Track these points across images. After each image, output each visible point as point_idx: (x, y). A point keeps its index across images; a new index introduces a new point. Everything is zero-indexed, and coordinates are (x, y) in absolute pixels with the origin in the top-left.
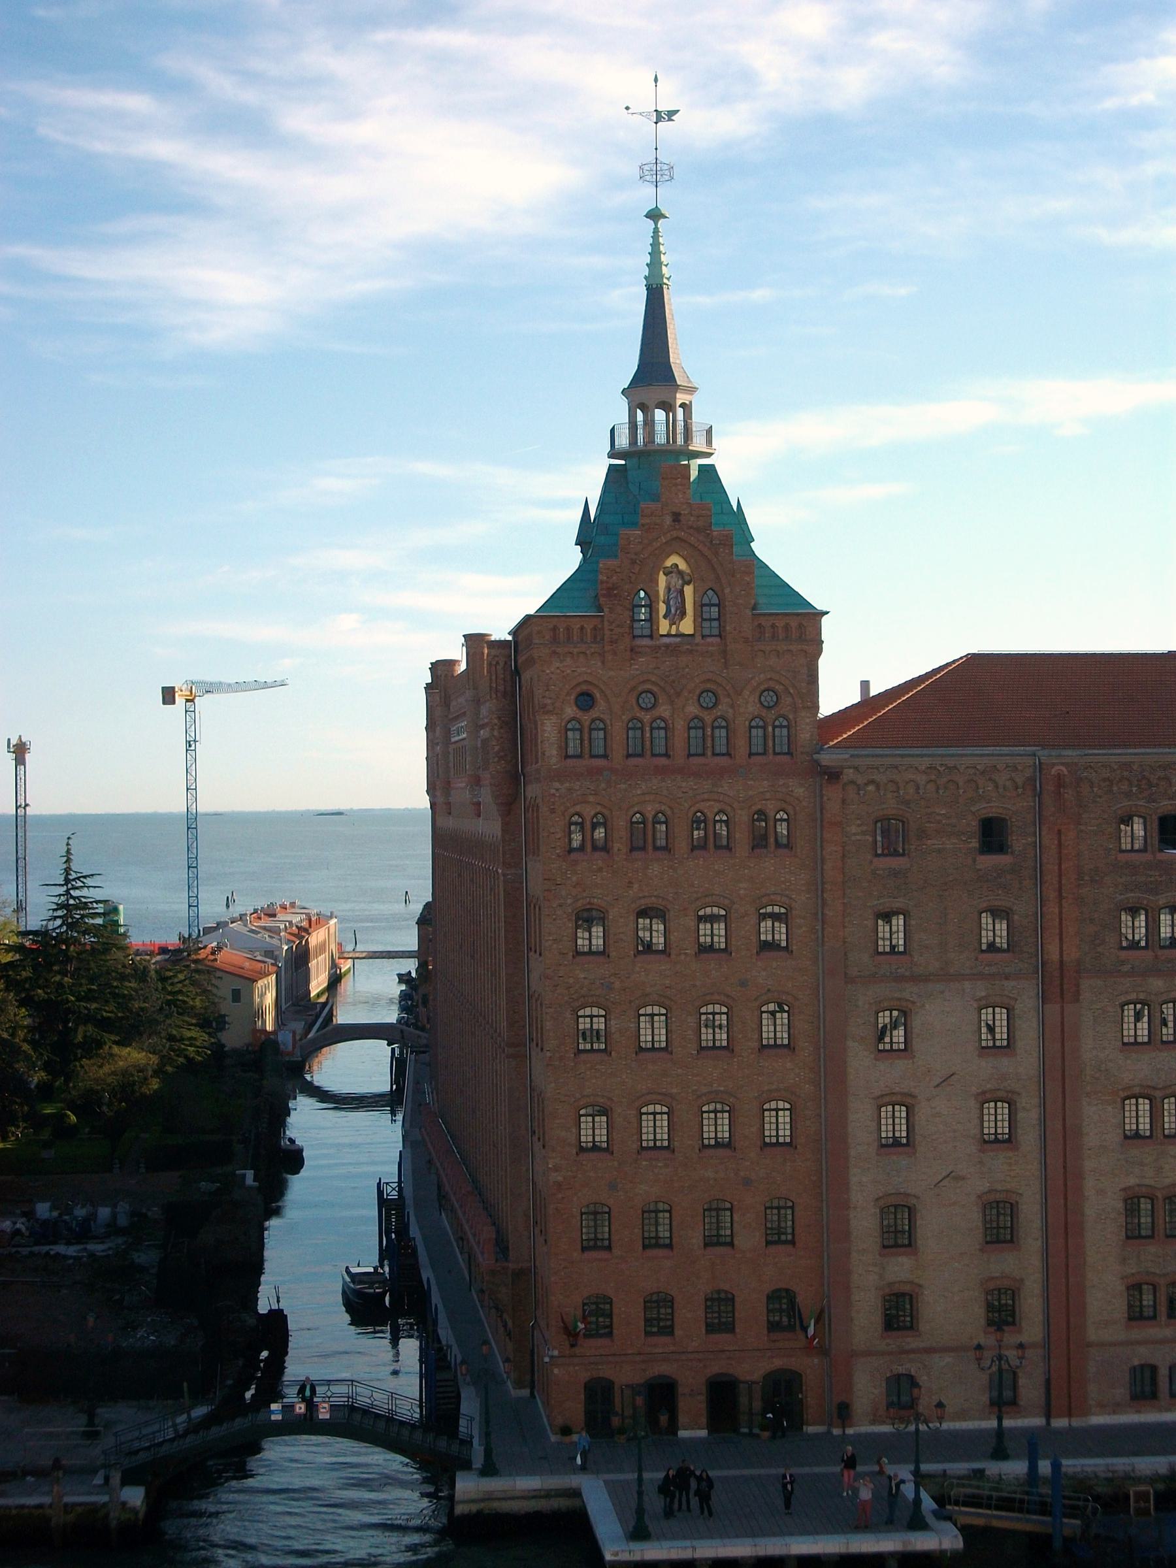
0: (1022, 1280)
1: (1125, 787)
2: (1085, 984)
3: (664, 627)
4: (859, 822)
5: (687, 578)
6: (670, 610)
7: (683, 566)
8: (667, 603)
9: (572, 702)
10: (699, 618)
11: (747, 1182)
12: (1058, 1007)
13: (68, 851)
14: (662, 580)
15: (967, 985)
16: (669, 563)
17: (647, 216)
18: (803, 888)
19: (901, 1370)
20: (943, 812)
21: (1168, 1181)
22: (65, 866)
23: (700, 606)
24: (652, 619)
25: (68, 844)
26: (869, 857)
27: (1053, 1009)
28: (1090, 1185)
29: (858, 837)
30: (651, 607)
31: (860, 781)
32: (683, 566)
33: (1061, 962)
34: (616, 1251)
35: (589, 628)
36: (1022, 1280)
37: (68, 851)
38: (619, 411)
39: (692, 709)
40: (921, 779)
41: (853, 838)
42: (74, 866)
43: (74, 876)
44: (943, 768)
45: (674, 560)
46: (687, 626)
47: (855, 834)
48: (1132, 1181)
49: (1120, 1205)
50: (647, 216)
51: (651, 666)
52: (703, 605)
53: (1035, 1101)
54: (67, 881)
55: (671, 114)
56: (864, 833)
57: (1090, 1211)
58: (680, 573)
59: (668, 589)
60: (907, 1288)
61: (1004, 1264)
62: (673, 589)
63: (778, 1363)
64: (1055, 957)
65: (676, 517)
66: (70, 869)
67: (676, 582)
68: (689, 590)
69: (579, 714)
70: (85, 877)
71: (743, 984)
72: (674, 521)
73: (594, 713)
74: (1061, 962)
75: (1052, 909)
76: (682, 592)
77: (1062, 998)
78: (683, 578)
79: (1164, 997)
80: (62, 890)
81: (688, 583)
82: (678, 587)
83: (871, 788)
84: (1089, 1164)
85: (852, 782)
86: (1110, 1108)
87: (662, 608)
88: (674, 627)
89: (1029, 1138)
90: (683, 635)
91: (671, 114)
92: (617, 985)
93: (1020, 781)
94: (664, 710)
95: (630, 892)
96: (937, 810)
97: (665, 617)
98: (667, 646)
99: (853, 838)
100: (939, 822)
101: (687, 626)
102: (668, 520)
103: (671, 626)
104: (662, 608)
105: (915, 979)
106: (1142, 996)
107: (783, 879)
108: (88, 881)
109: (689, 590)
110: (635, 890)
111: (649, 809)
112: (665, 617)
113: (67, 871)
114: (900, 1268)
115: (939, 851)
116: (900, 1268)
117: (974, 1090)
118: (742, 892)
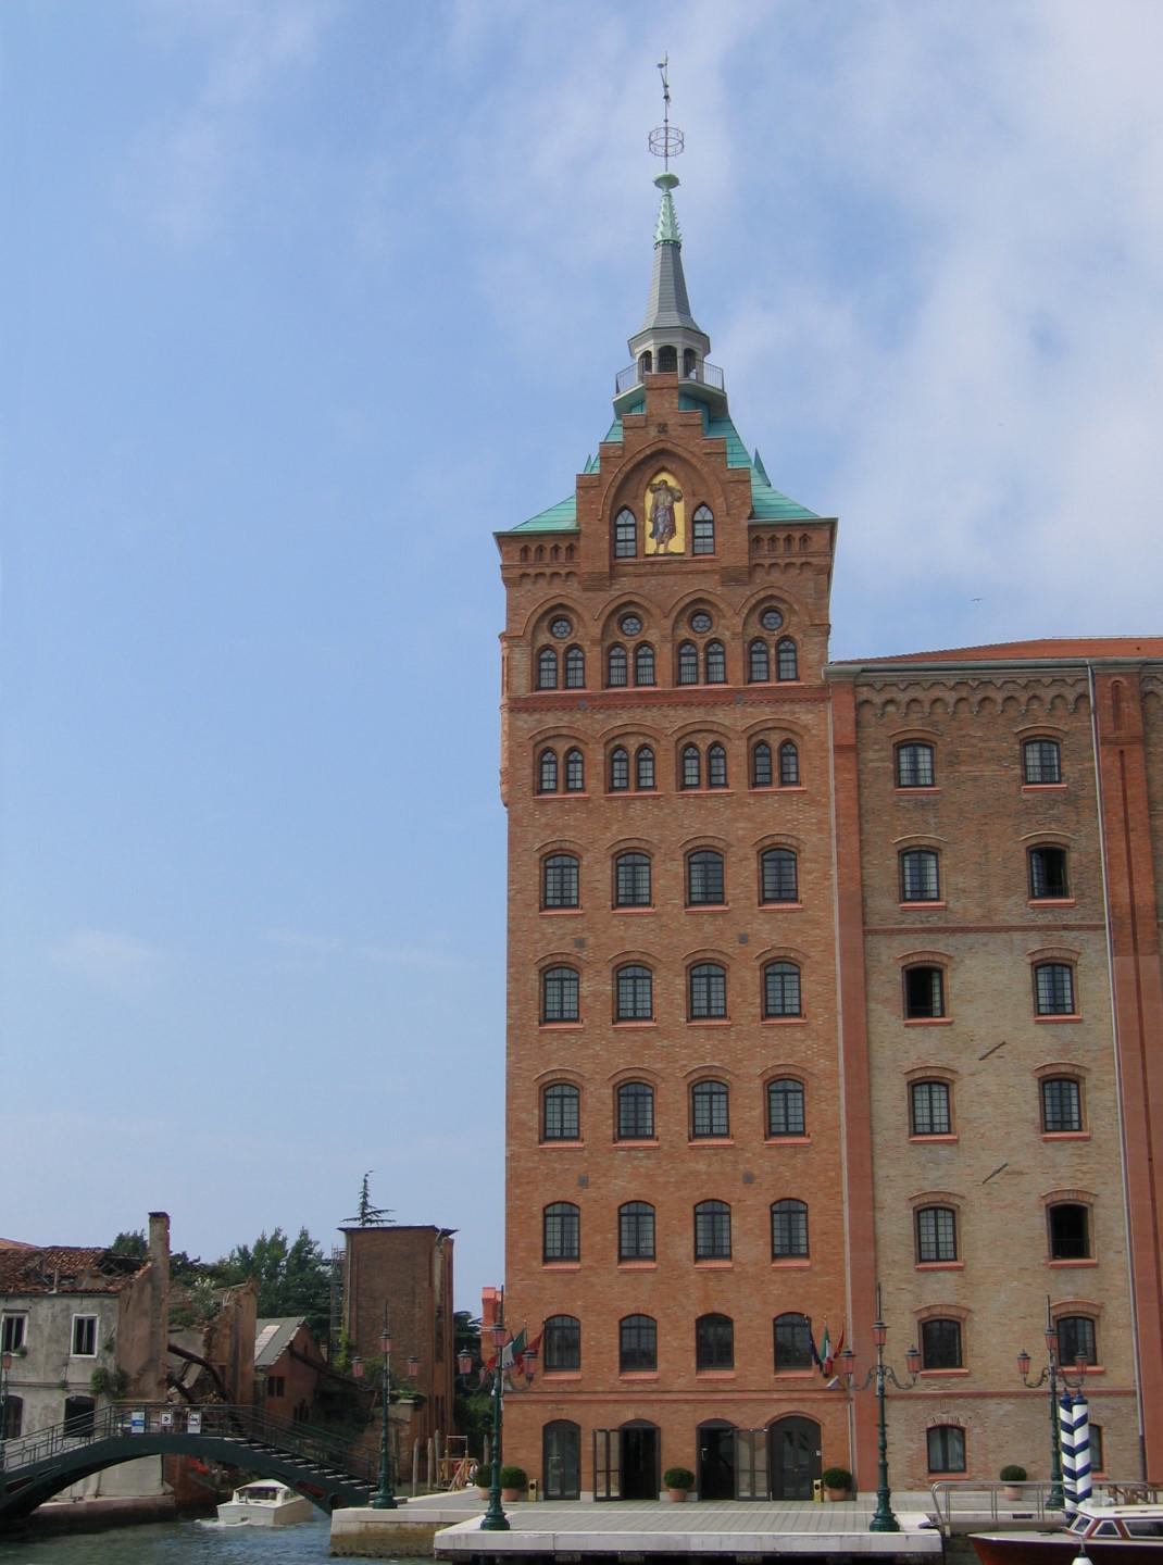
0: (1101, 1307)
3: (651, 546)
4: (877, 747)
5: (678, 494)
6: (658, 529)
7: (672, 482)
8: (654, 521)
9: (545, 628)
10: (692, 538)
11: (749, 1179)
13: (365, 1187)
14: (649, 498)
15: (1017, 936)
16: (656, 481)
17: (658, 182)
18: (814, 828)
19: (945, 1419)
20: (980, 734)
22: (361, 1200)
23: (692, 523)
24: (638, 540)
25: (365, 1181)
26: (890, 786)
29: (877, 764)
31: (878, 699)
32: (672, 482)
33: (1133, 908)
34: (585, 1261)
37: (365, 1187)
41: (871, 765)
42: (370, 1201)
43: (369, 1210)
44: (977, 683)
45: (664, 476)
46: (677, 544)
47: (872, 761)
50: (658, 182)
51: (634, 586)
52: (694, 522)
54: (364, 1215)
56: (882, 760)
58: (670, 490)
59: (656, 507)
62: (661, 507)
63: (786, 1408)
67: (665, 499)
68: (679, 508)
70: (379, 1212)
71: (744, 939)
72: (659, 432)
74: (1133, 908)
76: (671, 509)
77: (1136, 949)
78: (672, 495)
81: (679, 500)
82: (667, 504)
83: (891, 708)
85: (867, 702)
87: (649, 527)
88: (662, 546)
90: (672, 554)
92: (591, 941)
93: (1071, 695)
94: (652, 636)
95: (608, 834)
96: (971, 732)
97: (652, 536)
98: (653, 564)
99: (871, 765)
100: (974, 746)
101: (677, 544)
103: (658, 544)
104: (649, 527)
107: (789, 817)
109: (679, 508)
110: (614, 832)
111: (632, 742)
112: (652, 536)
113: (365, 1205)
114: (940, 1291)
115: (975, 779)
118: (740, 833)
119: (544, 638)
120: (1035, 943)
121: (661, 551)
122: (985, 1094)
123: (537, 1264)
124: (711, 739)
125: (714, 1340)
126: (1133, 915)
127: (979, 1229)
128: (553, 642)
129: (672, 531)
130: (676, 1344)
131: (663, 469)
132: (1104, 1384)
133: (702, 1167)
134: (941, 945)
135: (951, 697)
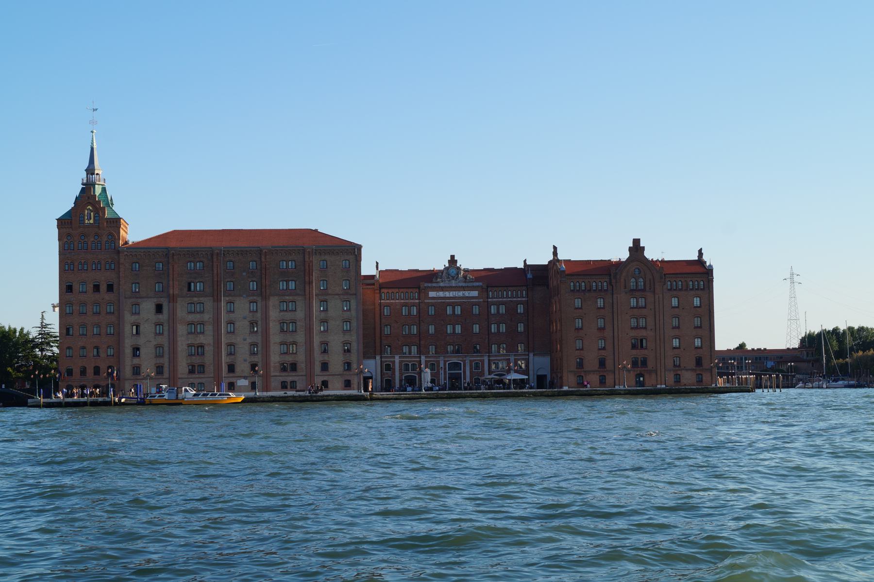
0: (164, 364)
1: (188, 256)
2: (179, 299)
3: (86, 221)
7: (91, 208)
8: (87, 216)
10: (94, 220)
14: (86, 211)
21: (197, 343)
23: (94, 217)
24: (84, 220)
25: (43, 315)
28: (179, 343)
30: (84, 217)
31: (128, 254)
32: (91, 208)
35: (69, 222)
36: (164, 364)
38: (84, 175)
39: (92, 239)
40: (142, 254)
42: (44, 321)
45: (89, 207)
46: (92, 221)
48: (189, 342)
49: (187, 348)
53: (167, 325)
55: (96, 109)
57: (179, 349)
59: (88, 213)
60: (138, 365)
61: (160, 361)
65: (89, 198)
66: (43, 322)
68: (92, 214)
70: (48, 325)
75: (171, 283)
79: (197, 302)
80: (40, 329)
83: (131, 256)
84: (179, 339)
85: (127, 255)
86: (184, 326)
87: (86, 217)
89: (166, 333)
91: (96, 109)
93: (164, 254)
94: (86, 240)
101: (92, 221)
102: (87, 198)
104: (86, 217)
105: (140, 298)
106: (192, 302)
108: (49, 326)
109: (92, 214)
116: (136, 361)
117: (154, 322)
119: (65, 240)
120: (155, 300)
122: (146, 328)
123: (65, 358)
124: (98, 261)
125: (97, 371)
127: (143, 351)
129: (91, 219)
130: (90, 371)
131: (88, 206)
132: (164, 377)
133: (95, 340)
134: (139, 300)
135: (142, 254)
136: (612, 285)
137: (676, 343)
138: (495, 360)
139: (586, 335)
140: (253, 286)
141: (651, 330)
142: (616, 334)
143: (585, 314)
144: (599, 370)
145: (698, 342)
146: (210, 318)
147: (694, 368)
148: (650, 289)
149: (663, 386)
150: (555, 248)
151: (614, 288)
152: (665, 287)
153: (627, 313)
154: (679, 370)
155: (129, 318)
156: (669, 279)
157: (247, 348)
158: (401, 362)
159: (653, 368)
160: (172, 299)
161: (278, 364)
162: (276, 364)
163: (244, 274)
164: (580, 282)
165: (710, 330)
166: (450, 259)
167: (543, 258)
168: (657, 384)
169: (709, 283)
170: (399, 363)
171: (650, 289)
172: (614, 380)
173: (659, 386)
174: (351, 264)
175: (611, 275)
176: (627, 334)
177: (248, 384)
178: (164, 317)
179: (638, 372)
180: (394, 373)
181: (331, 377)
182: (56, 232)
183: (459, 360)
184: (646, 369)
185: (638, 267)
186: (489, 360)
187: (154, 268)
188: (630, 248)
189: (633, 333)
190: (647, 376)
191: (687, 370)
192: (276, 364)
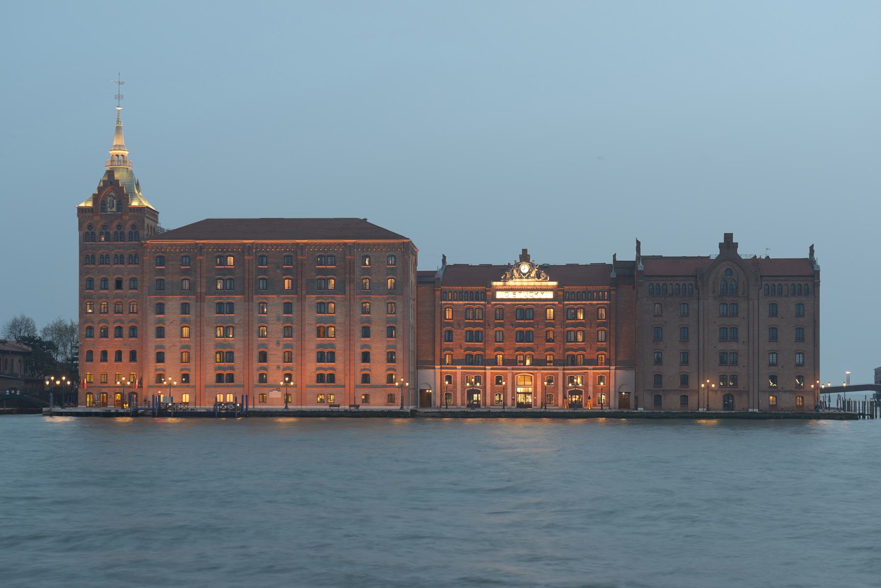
8: (110, 204)
10: (118, 210)
12: (199, 303)
14: (109, 198)
23: (117, 204)
27: (198, 304)
32: (114, 195)
45: (112, 193)
46: (114, 209)
58: (113, 197)
64: (199, 291)
68: (115, 201)
69: (88, 231)
73: (92, 231)
76: (113, 201)
81: (115, 199)
87: (109, 205)
94: (108, 230)
102: (109, 183)
104: (109, 205)
109: (115, 201)
119: (86, 230)
121: (111, 211)
126: (201, 294)
128: (88, 231)
129: (113, 207)
136: (698, 289)
137: (773, 358)
138: (570, 373)
139: (665, 347)
140: (287, 284)
141: (744, 342)
142: (701, 346)
143: (665, 322)
144: (681, 389)
145: (799, 359)
146: (240, 320)
147: (794, 389)
148: (743, 294)
149: (756, 410)
150: (638, 243)
151: (701, 292)
152: (762, 291)
153: (715, 323)
154: (776, 392)
155: (152, 317)
156: (766, 282)
157: (280, 354)
158: (463, 374)
159: (744, 388)
160: (200, 299)
161: (314, 374)
162: (312, 374)
163: (278, 271)
164: (661, 285)
165: (814, 345)
166: (521, 254)
167: (628, 255)
168: (749, 408)
169: (814, 287)
170: (462, 374)
171: (743, 294)
172: (697, 401)
173: (750, 410)
174: (397, 260)
175: (697, 276)
176: (715, 347)
177: (280, 397)
178: (191, 316)
179: (727, 393)
180: (455, 387)
181: (372, 390)
182: (76, 220)
183: (529, 373)
184: (736, 389)
185: (730, 267)
186: (564, 374)
187: (181, 263)
188: (721, 245)
189: (722, 347)
190: (736, 398)
191: (785, 392)
192: (312, 374)
